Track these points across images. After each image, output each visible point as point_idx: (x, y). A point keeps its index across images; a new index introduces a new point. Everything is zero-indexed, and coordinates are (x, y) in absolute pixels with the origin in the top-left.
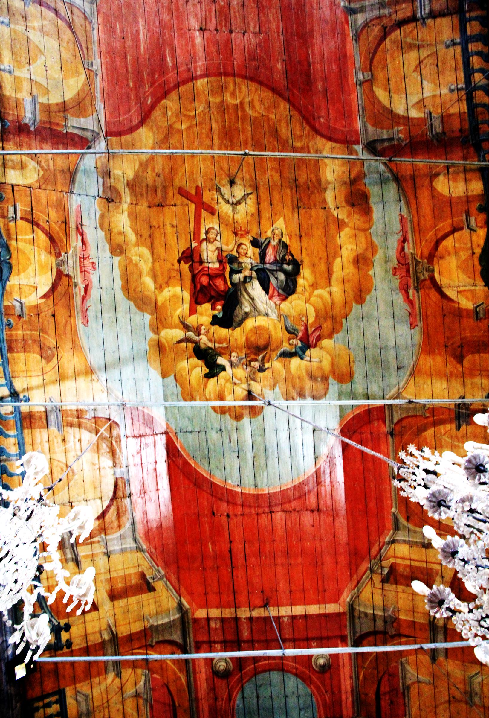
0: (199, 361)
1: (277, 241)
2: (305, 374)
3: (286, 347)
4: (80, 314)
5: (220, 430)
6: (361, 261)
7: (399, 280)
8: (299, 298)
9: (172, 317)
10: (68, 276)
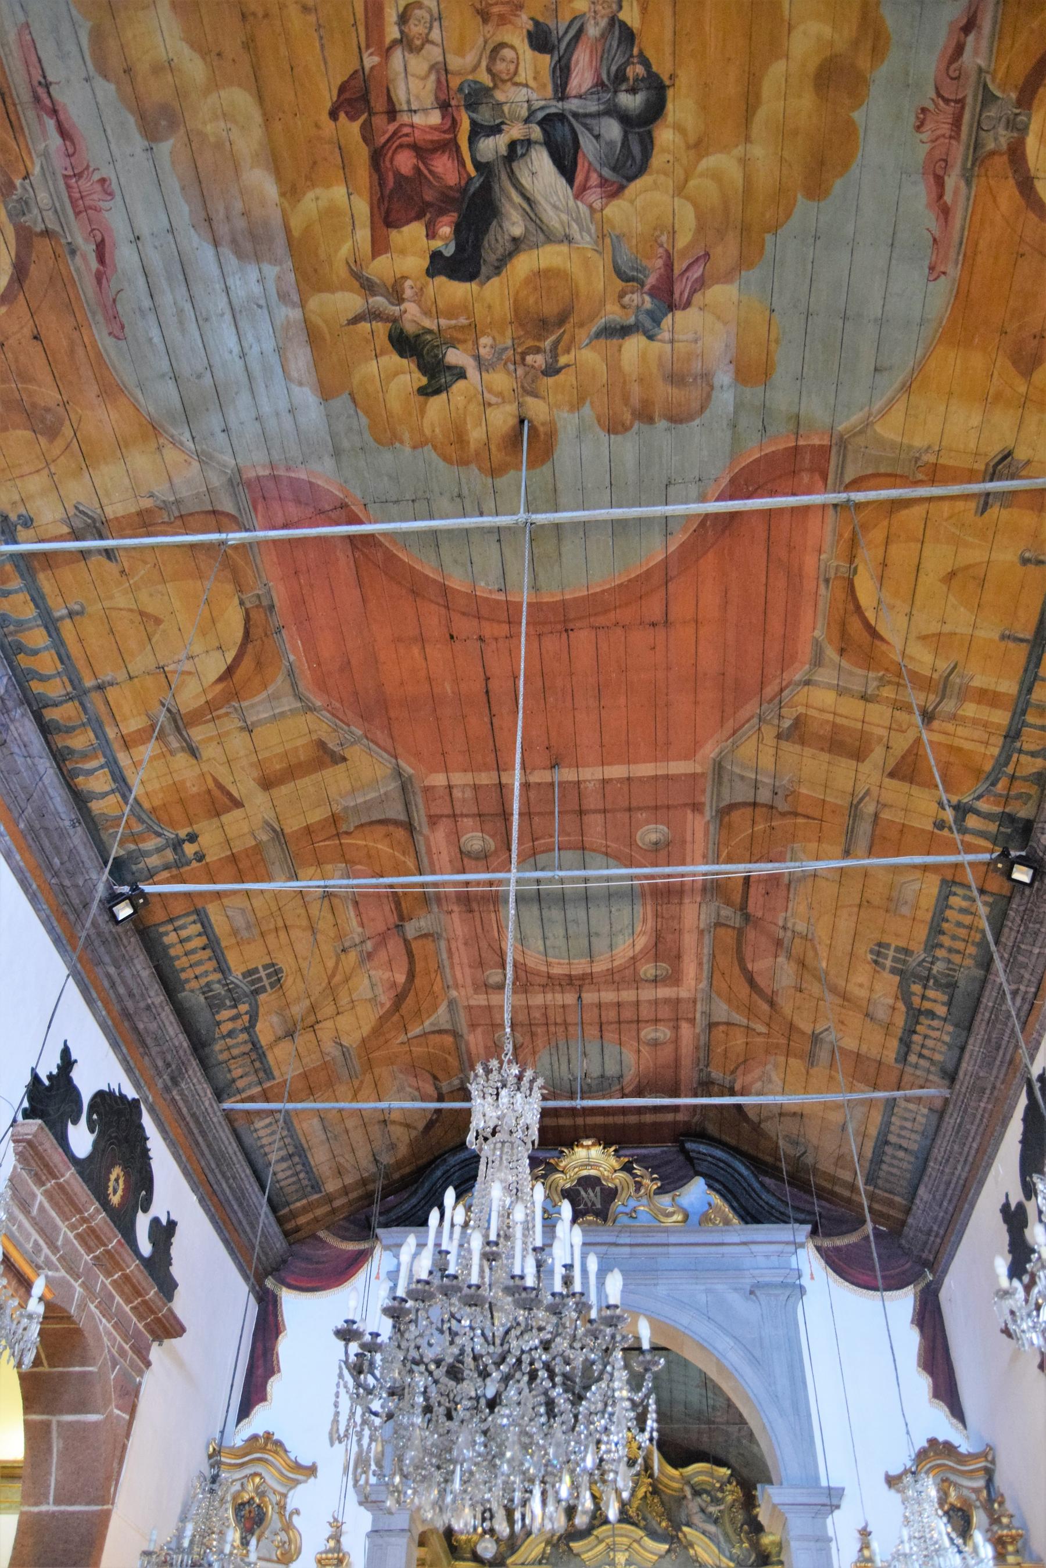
0: (405, 361)
1: (603, 23)
2: (655, 371)
3: (612, 313)
4: (100, 317)
5: (459, 496)
6: (836, 79)
7: (927, 147)
8: (656, 186)
9: (331, 265)
10: (47, 233)
